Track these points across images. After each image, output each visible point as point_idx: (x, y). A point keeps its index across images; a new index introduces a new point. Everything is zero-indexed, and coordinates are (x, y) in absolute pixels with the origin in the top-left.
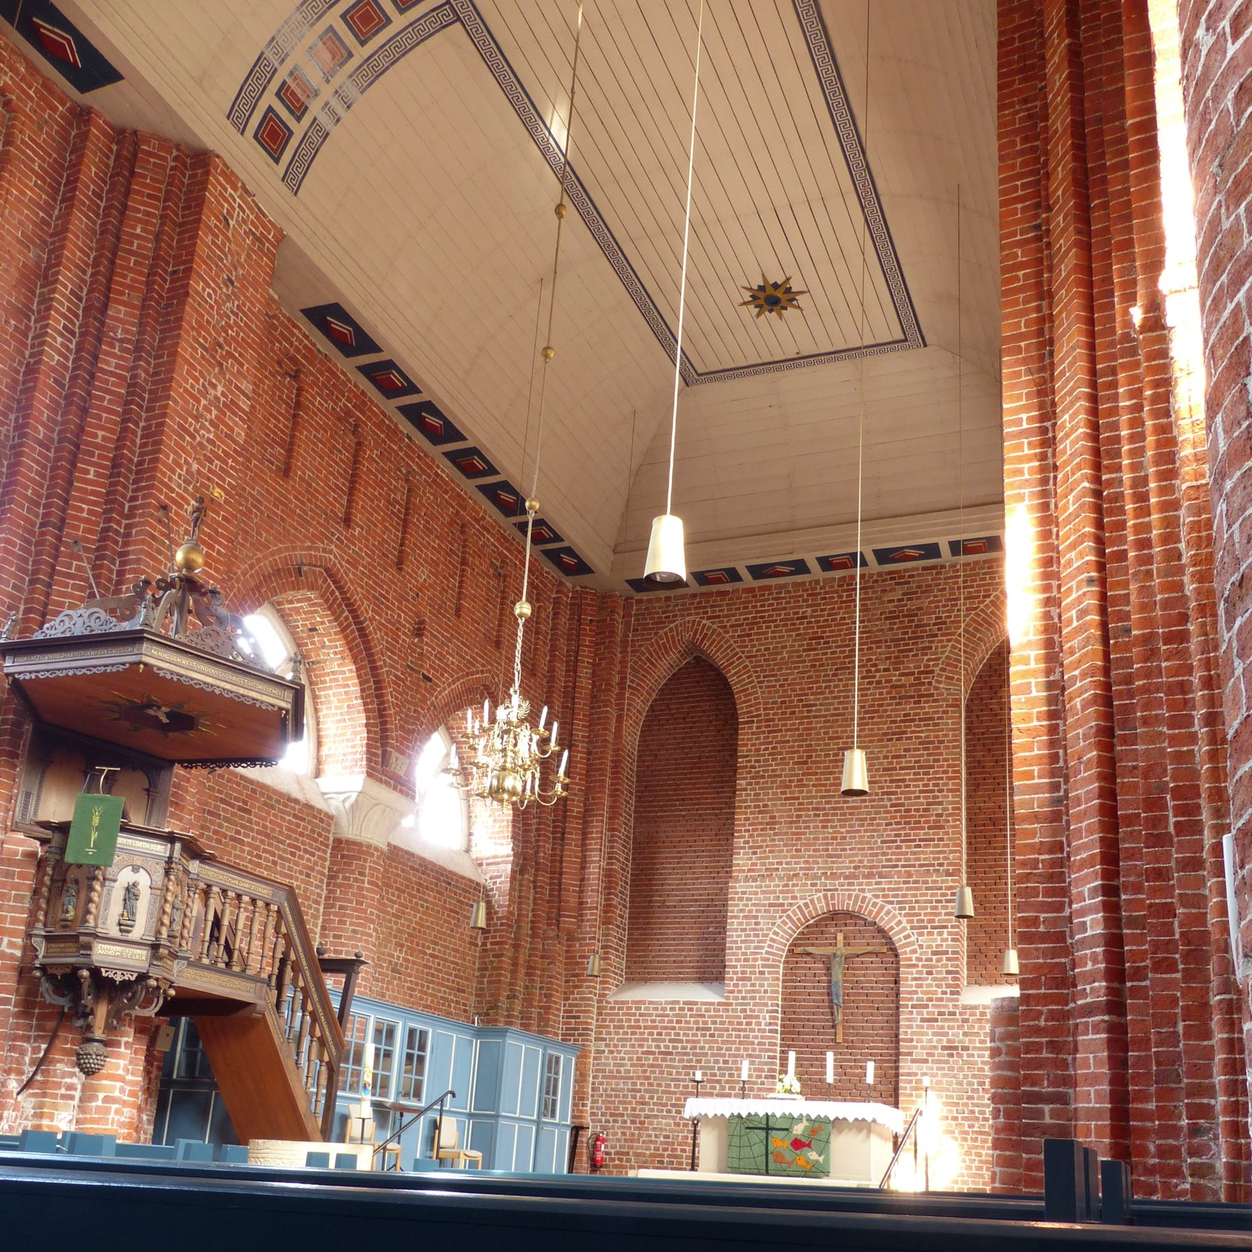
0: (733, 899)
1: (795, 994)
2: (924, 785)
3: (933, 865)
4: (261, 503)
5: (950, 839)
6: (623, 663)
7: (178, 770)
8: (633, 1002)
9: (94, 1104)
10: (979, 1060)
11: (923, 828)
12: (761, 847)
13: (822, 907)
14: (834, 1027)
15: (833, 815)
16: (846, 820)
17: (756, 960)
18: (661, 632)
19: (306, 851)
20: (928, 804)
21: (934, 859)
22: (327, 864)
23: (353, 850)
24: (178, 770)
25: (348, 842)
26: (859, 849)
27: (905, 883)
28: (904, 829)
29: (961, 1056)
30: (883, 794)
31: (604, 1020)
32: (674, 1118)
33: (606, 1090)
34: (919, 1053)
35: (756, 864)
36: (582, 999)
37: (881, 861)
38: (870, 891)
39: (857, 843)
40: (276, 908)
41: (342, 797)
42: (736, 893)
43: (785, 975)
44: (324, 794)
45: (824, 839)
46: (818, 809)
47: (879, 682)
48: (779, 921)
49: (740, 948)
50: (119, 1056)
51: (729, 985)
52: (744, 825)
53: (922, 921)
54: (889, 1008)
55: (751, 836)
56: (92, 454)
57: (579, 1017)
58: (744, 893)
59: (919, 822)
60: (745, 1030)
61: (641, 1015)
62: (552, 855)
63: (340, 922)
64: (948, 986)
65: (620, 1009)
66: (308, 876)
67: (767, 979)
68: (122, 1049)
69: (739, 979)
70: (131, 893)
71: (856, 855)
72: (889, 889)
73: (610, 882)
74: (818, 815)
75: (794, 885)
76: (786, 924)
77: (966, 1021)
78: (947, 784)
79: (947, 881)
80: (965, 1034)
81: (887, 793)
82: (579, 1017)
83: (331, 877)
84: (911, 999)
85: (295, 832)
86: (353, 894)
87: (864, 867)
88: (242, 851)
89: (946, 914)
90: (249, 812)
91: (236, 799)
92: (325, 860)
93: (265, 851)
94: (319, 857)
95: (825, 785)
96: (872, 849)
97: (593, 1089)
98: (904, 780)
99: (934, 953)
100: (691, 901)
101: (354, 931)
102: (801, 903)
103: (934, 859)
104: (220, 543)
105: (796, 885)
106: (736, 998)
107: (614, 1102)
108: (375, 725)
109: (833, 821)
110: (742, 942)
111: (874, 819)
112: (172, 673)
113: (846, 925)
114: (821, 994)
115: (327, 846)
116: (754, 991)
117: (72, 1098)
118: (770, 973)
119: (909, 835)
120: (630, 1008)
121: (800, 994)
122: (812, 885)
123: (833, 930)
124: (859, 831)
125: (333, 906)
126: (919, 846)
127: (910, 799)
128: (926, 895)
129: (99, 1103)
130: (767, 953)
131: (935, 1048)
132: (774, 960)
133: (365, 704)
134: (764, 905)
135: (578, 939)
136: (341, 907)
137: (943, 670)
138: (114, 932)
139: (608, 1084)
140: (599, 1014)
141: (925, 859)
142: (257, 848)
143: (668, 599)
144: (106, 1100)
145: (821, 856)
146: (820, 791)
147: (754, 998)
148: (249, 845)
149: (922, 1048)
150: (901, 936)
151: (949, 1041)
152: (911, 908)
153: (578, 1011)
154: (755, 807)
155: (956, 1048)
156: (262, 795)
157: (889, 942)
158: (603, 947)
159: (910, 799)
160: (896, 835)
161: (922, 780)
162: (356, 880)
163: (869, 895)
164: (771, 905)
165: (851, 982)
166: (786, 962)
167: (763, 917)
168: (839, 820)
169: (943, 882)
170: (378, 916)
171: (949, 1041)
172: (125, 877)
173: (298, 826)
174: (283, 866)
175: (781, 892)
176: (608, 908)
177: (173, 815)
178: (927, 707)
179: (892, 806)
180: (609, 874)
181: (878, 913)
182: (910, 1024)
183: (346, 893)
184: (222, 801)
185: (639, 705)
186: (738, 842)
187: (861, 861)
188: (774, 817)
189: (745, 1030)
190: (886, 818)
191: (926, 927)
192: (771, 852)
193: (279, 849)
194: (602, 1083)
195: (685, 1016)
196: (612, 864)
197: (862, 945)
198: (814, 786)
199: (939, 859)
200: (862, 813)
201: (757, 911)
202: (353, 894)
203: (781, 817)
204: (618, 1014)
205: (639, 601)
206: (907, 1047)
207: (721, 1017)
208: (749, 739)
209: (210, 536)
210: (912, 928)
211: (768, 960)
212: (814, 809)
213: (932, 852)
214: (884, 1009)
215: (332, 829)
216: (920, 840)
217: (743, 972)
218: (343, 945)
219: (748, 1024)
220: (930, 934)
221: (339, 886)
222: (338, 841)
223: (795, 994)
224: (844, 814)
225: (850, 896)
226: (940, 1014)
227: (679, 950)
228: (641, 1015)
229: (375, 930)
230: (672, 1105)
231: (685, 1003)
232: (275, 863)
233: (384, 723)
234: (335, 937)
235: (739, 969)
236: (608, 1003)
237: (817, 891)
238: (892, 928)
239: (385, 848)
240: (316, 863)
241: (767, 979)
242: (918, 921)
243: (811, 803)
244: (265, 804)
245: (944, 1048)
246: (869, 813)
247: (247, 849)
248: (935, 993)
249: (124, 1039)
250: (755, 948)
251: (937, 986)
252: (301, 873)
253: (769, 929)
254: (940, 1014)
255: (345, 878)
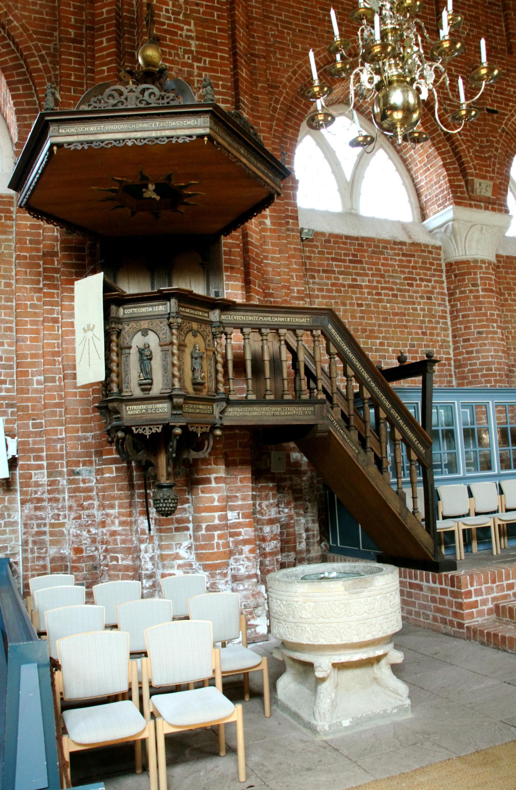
4: (291, 23)
7: (224, 240)
9: (200, 533)
19: (421, 280)
22: (445, 285)
23: (463, 268)
24: (224, 240)
25: (457, 263)
40: (319, 332)
41: (443, 229)
44: (431, 232)
50: (211, 491)
56: (102, 28)
63: (466, 328)
66: (429, 298)
68: (213, 484)
70: (145, 356)
83: (450, 295)
85: (408, 267)
86: (471, 303)
88: (362, 293)
90: (360, 262)
91: (345, 255)
92: (443, 282)
93: (383, 288)
94: (436, 281)
101: (479, 333)
104: (221, 51)
108: (451, 164)
112: (82, 143)
115: (441, 271)
117: (187, 529)
125: (457, 317)
129: (204, 532)
133: (438, 149)
136: (464, 316)
138: (137, 393)
142: (376, 288)
144: (208, 528)
148: (367, 287)
156: (369, 246)
162: (471, 291)
170: (498, 315)
172: (138, 341)
173: (410, 262)
174: (404, 296)
177: (229, 278)
183: (465, 304)
184: (333, 259)
193: (395, 283)
202: (471, 303)
209: (209, 48)
215: (442, 256)
218: (472, 346)
221: (459, 299)
222: (449, 265)
229: (498, 327)
232: (395, 296)
233: (459, 159)
234: (465, 341)
239: (494, 260)
240: (434, 287)
244: (374, 252)
247: (366, 291)
249: (213, 476)
252: (422, 297)
255: (461, 292)
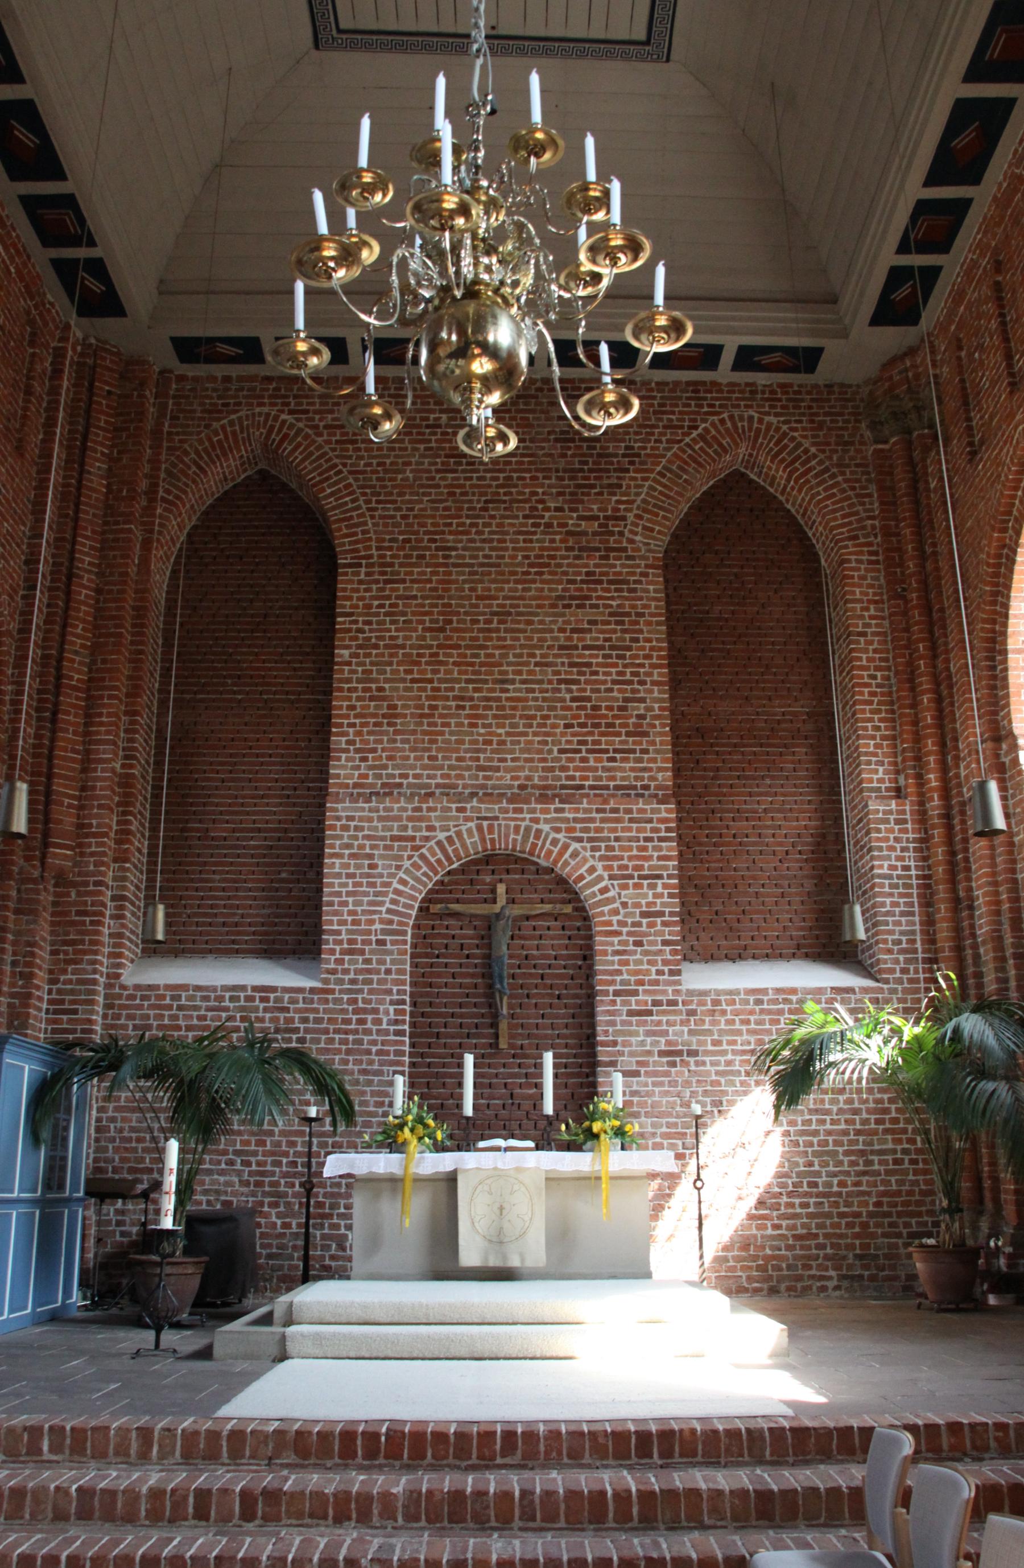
0: (333, 827)
1: (432, 975)
2: (619, 673)
3: (635, 788)
5: (657, 751)
6: (155, 463)
8: (168, 987)
10: (713, 1069)
11: (619, 734)
12: (374, 750)
13: (473, 844)
14: (494, 1025)
15: (485, 708)
16: (505, 717)
17: (371, 922)
18: (215, 425)
20: (626, 700)
21: (636, 778)
26: (526, 760)
27: (598, 811)
28: (592, 734)
29: (688, 1064)
30: (560, 682)
31: (118, 1017)
32: (239, 1173)
33: (121, 1130)
34: (628, 1062)
35: (366, 776)
36: (80, 982)
37: (559, 779)
38: (546, 821)
39: (522, 751)
42: (339, 818)
43: (414, 946)
45: (471, 742)
46: (462, 698)
47: (549, 525)
48: (407, 864)
49: (345, 904)
51: (328, 961)
52: (348, 717)
53: (626, 867)
54: (576, 996)
55: (359, 733)
57: (75, 1012)
58: (350, 818)
59: (613, 725)
60: (356, 1032)
61: (180, 1008)
62: (34, 746)
64: (665, 962)
65: (144, 998)
67: (390, 953)
69: (343, 952)
71: (521, 769)
72: (575, 820)
73: (126, 795)
74: (463, 708)
75: (429, 809)
76: (419, 868)
77: (692, 1013)
78: (650, 674)
79: (659, 811)
80: (691, 1032)
81: (567, 682)
82: (75, 1012)
84: (613, 982)
87: (533, 787)
89: (659, 858)
95: (472, 664)
96: (544, 760)
97: (98, 1130)
98: (589, 665)
99: (644, 915)
100: (252, 830)
102: (442, 836)
103: (636, 778)
105: (435, 809)
106: (341, 982)
107: (135, 1150)
109: (485, 717)
110: (349, 894)
111: (548, 717)
113: (508, 872)
114: (473, 976)
116: (369, 971)
118: (394, 943)
119: (599, 743)
120: (163, 997)
121: (439, 975)
122: (459, 810)
123: (488, 879)
124: (526, 734)
126: (613, 759)
127: (598, 691)
128: (630, 830)
130: (389, 911)
131: (649, 1053)
132: (400, 923)
134: (383, 838)
135: (74, 884)
137: (639, 517)
139: (124, 1120)
140: (108, 1006)
141: (623, 779)
143: (227, 379)
145: (469, 768)
146: (466, 672)
147: (370, 982)
149: (632, 1054)
150: (596, 889)
151: (668, 1043)
152: (608, 848)
153: (73, 1002)
154: (365, 690)
155: (679, 1053)
157: (573, 897)
158: (113, 898)
159: (598, 691)
160: (580, 743)
161: (616, 665)
163: (546, 828)
164: (393, 838)
165: (518, 957)
166: (417, 926)
167: (382, 857)
168: (495, 717)
169: (653, 811)
171: (668, 1043)
175: (410, 819)
176: (124, 835)
178: (619, 566)
179: (574, 699)
180: (126, 782)
181: (561, 854)
182: (611, 1018)
185: (176, 528)
186: (339, 741)
187: (528, 778)
188: (395, 707)
189: (356, 1032)
190: (565, 717)
191: (631, 877)
192: (390, 758)
194: (113, 1120)
195: (256, 1009)
196: (131, 766)
197: (531, 902)
198: (455, 664)
199: (642, 779)
200: (529, 708)
201: (372, 847)
203: (404, 707)
204: (140, 1007)
205: (181, 378)
206: (608, 1053)
207: (316, 1011)
208: (352, 590)
210: (611, 878)
211: (390, 922)
212: (456, 698)
213: (632, 769)
214: (568, 996)
216: (615, 751)
217: (350, 942)
219: (361, 1022)
220: (637, 886)
223: (432, 975)
224: (502, 708)
225: (517, 828)
226: (655, 1003)
227: (231, 907)
228: (180, 1008)
230: (236, 1153)
231: (255, 989)
235: (344, 936)
236: (123, 987)
237: (467, 819)
238: (581, 877)
241: (390, 953)
242: (620, 868)
243: (452, 689)
245: (662, 1054)
246: (539, 708)
248: (648, 972)
250: (371, 903)
251: (649, 962)
253: (392, 875)
254: (655, 1003)
